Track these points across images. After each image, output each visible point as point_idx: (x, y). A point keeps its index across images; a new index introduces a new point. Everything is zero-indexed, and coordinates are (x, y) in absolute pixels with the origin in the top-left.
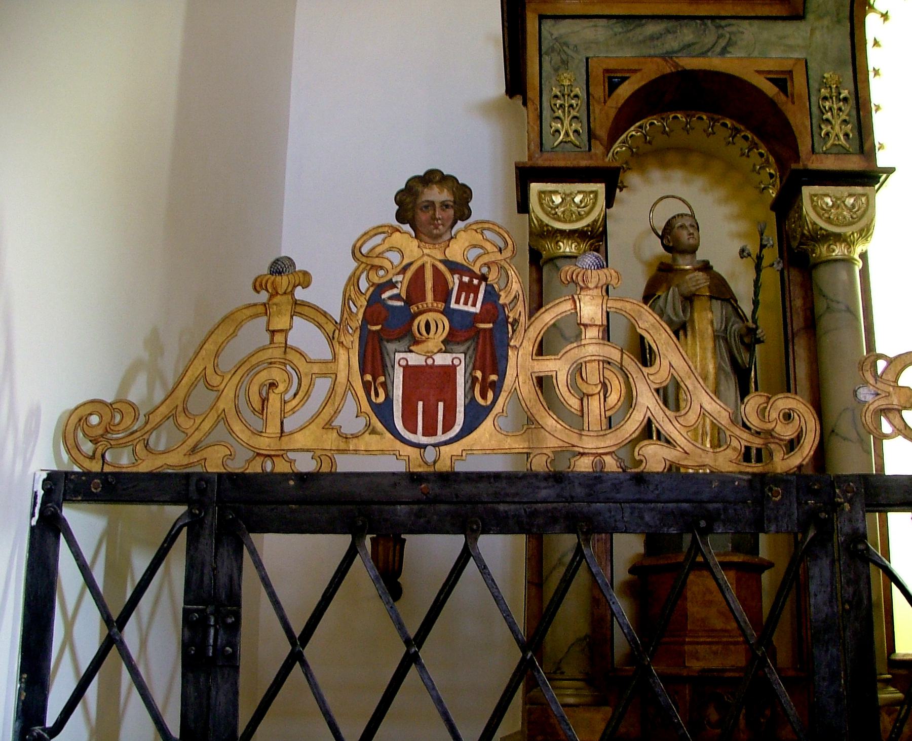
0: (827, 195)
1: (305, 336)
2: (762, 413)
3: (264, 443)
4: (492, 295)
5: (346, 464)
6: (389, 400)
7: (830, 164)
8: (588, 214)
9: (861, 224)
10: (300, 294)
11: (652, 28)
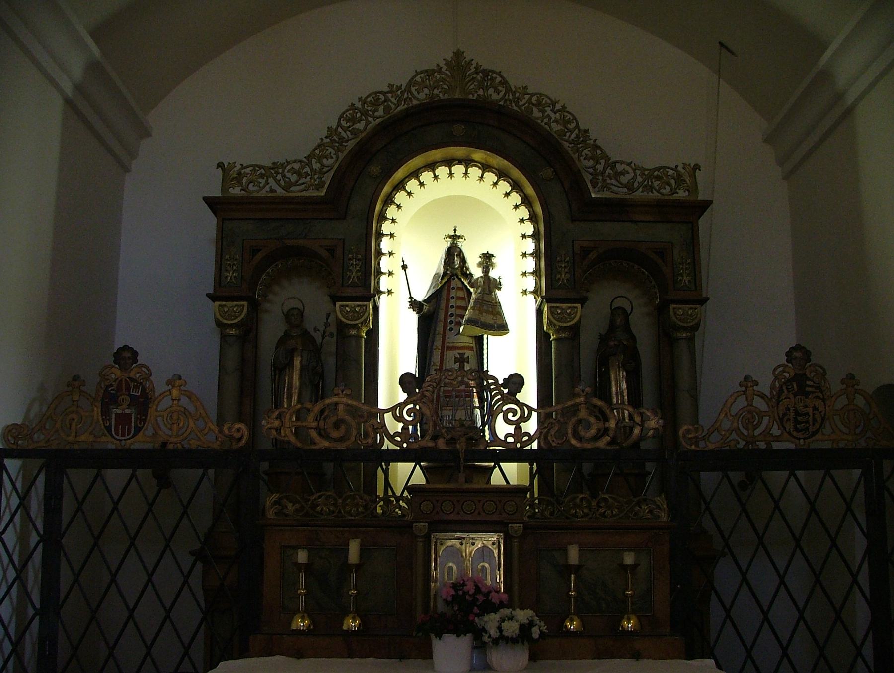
2: (230, 429)
3: (70, 439)
4: (144, 389)
6: (110, 425)
7: (349, 292)
10: (82, 388)
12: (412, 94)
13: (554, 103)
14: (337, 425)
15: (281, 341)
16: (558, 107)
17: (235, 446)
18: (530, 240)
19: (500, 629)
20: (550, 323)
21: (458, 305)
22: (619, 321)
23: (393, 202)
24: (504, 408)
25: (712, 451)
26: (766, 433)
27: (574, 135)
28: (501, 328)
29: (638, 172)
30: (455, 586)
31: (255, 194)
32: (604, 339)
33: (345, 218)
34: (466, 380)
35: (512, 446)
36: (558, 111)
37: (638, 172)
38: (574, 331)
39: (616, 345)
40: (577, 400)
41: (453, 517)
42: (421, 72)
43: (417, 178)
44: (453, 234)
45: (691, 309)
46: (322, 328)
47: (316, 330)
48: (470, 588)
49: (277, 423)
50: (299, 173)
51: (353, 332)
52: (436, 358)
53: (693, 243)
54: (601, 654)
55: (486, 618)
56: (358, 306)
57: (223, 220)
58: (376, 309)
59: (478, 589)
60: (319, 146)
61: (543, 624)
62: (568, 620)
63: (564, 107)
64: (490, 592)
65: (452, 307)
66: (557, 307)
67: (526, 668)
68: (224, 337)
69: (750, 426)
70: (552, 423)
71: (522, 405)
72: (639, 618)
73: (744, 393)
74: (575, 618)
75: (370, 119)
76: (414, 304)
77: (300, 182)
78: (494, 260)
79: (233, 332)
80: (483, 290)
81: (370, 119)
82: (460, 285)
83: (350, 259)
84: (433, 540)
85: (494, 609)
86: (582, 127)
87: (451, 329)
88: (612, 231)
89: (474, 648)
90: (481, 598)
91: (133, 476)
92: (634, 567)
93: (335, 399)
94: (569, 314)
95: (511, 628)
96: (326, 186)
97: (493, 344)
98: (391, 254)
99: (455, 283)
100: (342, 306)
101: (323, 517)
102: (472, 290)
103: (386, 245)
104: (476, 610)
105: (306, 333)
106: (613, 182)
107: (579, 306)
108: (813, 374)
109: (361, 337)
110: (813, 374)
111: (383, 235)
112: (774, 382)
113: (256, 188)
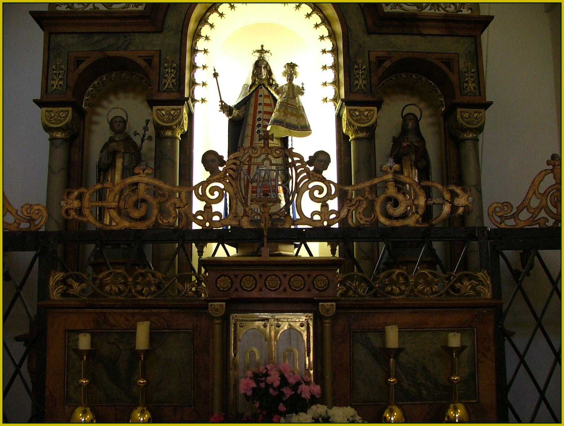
0: (163, 110)
7: (165, 96)
8: (64, 120)
9: (177, 122)
11: (96, 38)
14: (136, 205)
15: (106, 146)
18: (330, 55)
20: (349, 124)
23: (206, 22)
24: (311, 186)
25: (522, 229)
30: (256, 377)
32: (396, 142)
33: (161, 31)
34: (270, 156)
35: (319, 225)
38: (371, 130)
39: (407, 147)
40: (386, 177)
41: (255, 294)
44: (260, 49)
45: (475, 112)
46: (141, 132)
47: (136, 134)
48: (274, 379)
49: (76, 204)
51: (169, 133)
53: (476, 55)
56: (173, 109)
57: (50, 34)
58: (191, 116)
59: (284, 380)
62: (387, 410)
64: (298, 384)
65: (260, 112)
66: (357, 110)
68: (52, 140)
70: (360, 201)
72: (464, 404)
73: (552, 171)
74: (395, 408)
76: (225, 108)
79: (59, 135)
80: (288, 95)
82: (266, 93)
83: (166, 68)
84: (232, 321)
88: (404, 44)
90: (288, 392)
92: (462, 349)
93: (135, 179)
94: (367, 116)
98: (204, 67)
99: (262, 91)
100: (158, 110)
101: (111, 297)
102: (277, 97)
103: (199, 59)
104: (282, 408)
105: (128, 139)
107: (375, 109)
109: (176, 138)
111: (197, 51)
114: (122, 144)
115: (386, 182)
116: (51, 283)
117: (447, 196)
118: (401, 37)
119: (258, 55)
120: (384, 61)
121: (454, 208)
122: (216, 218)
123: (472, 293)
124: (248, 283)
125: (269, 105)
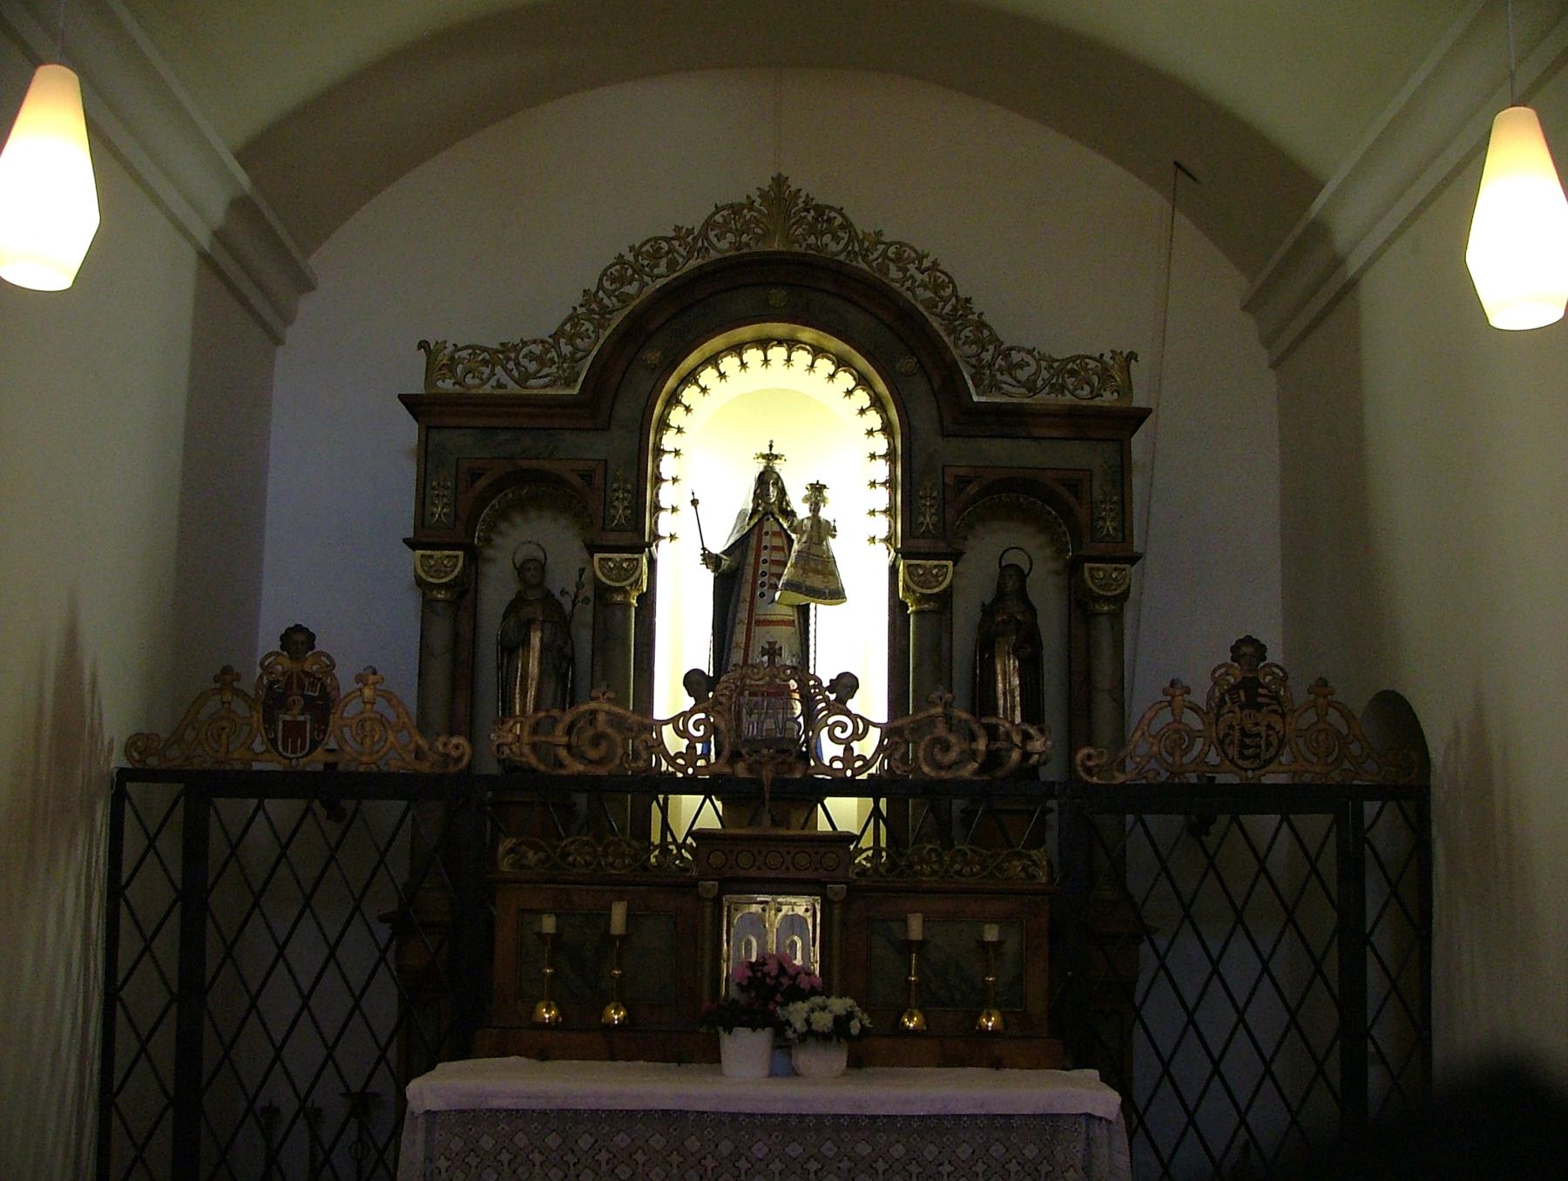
1: (240, 707)
2: (445, 745)
4: (323, 687)
5: (256, 766)
7: (612, 538)
12: (708, 239)
13: (921, 257)
14: (596, 741)
15: (513, 608)
16: (926, 263)
17: (452, 769)
19: (808, 1021)
20: (907, 588)
21: (772, 560)
22: (1011, 584)
24: (830, 721)
26: (1201, 760)
27: (948, 307)
28: (836, 595)
29: (1043, 364)
31: (473, 391)
32: (988, 612)
33: (607, 428)
35: (840, 775)
36: (928, 269)
37: (1043, 364)
38: (944, 601)
40: (933, 711)
41: (753, 873)
42: (724, 208)
43: (717, 367)
46: (572, 589)
47: (563, 592)
48: (772, 968)
50: (540, 360)
51: (619, 598)
52: (740, 637)
53: (1122, 470)
54: (950, 1060)
55: (791, 1007)
57: (428, 428)
58: (652, 563)
59: (782, 970)
60: (570, 318)
61: (865, 1016)
63: (935, 264)
64: (798, 974)
65: (765, 561)
67: (844, 1074)
68: (428, 603)
69: (1178, 753)
71: (854, 717)
72: (1003, 1015)
73: (1170, 703)
75: (646, 279)
76: (709, 559)
77: (543, 373)
78: (826, 493)
80: (810, 537)
81: (646, 279)
82: (776, 528)
84: (726, 904)
85: (803, 996)
86: (962, 294)
87: (762, 595)
89: (775, 1047)
90: (785, 981)
91: (308, 810)
92: (1000, 943)
93: (593, 705)
94: (937, 576)
95: (823, 1021)
96: (581, 379)
97: (823, 616)
99: (770, 525)
102: (794, 536)
103: (668, 466)
104: (779, 998)
105: (548, 597)
106: (1006, 378)
108: (1268, 678)
109: (630, 605)
110: (1268, 678)
111: (664, 452)
112: (1212, 690)
113: (477, 381)
114: (534, 596)
115: (932, 718)
116: (501, 849)
117: (1017, 739)
118: (998, 442)
119: (763, 462)
120: (969, 482)
121: (1026, 755)
122: (701, 763)
123: (1023, 875)
124: (744, 860)
125: (782, 549)
